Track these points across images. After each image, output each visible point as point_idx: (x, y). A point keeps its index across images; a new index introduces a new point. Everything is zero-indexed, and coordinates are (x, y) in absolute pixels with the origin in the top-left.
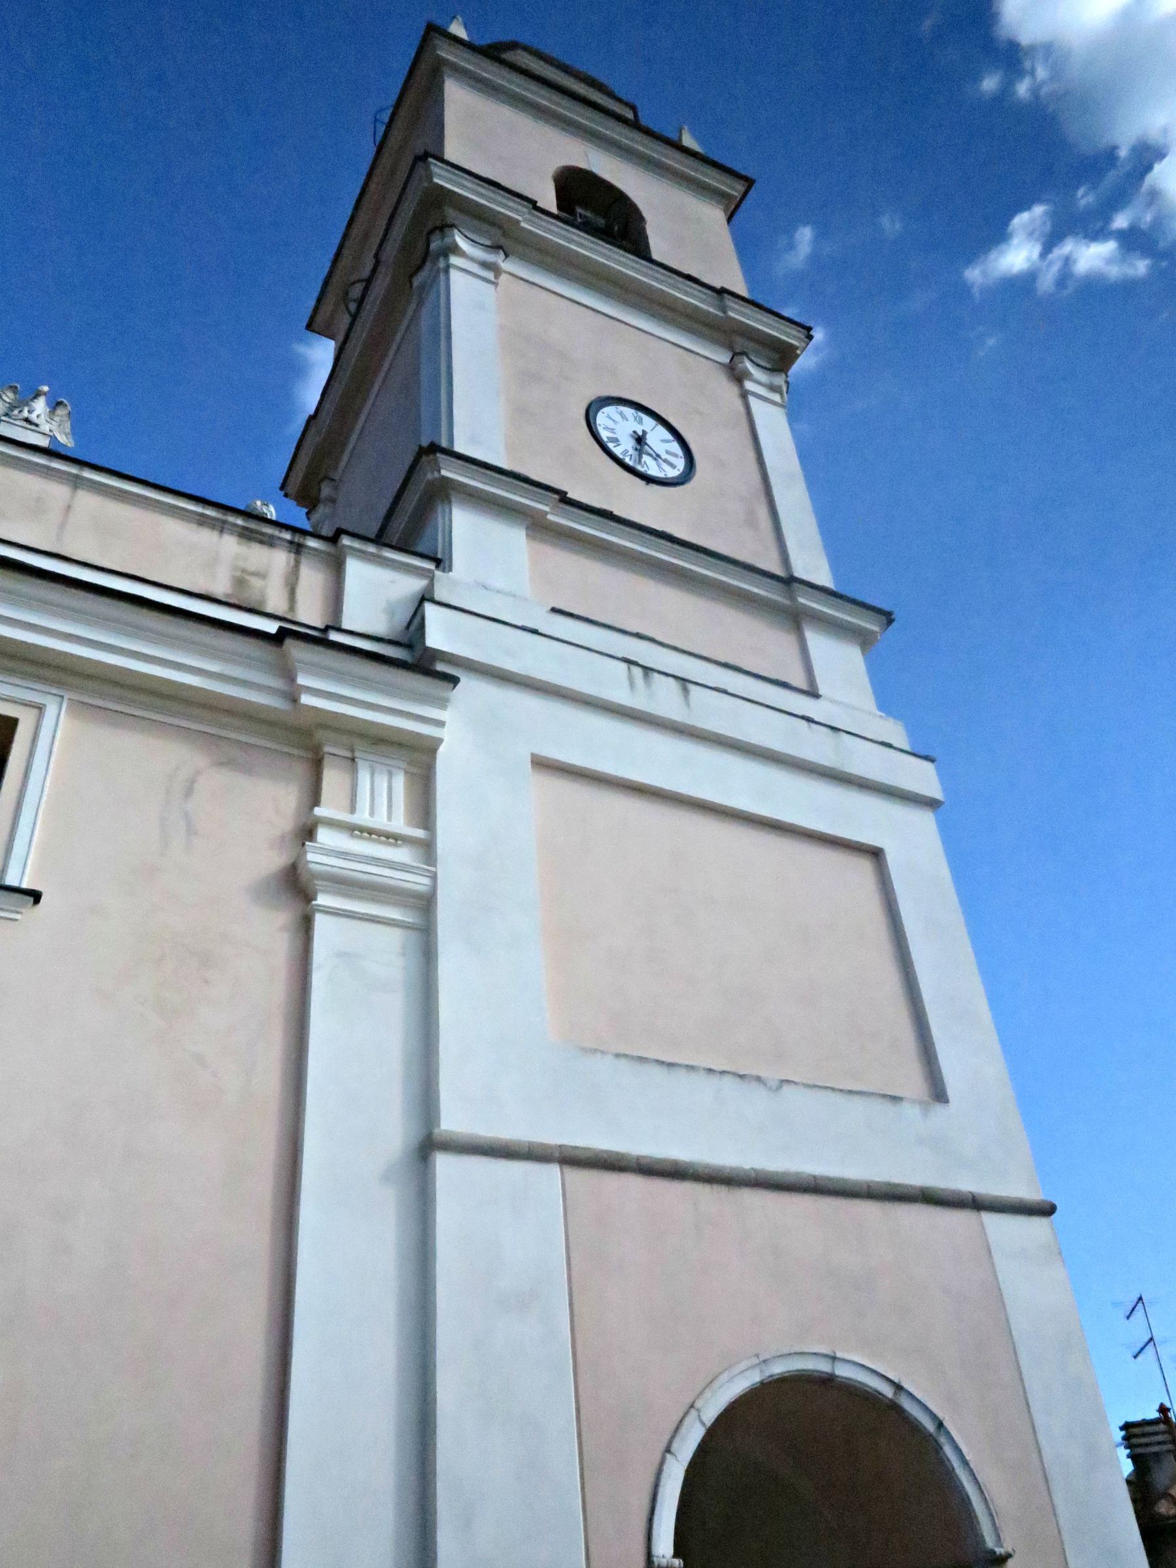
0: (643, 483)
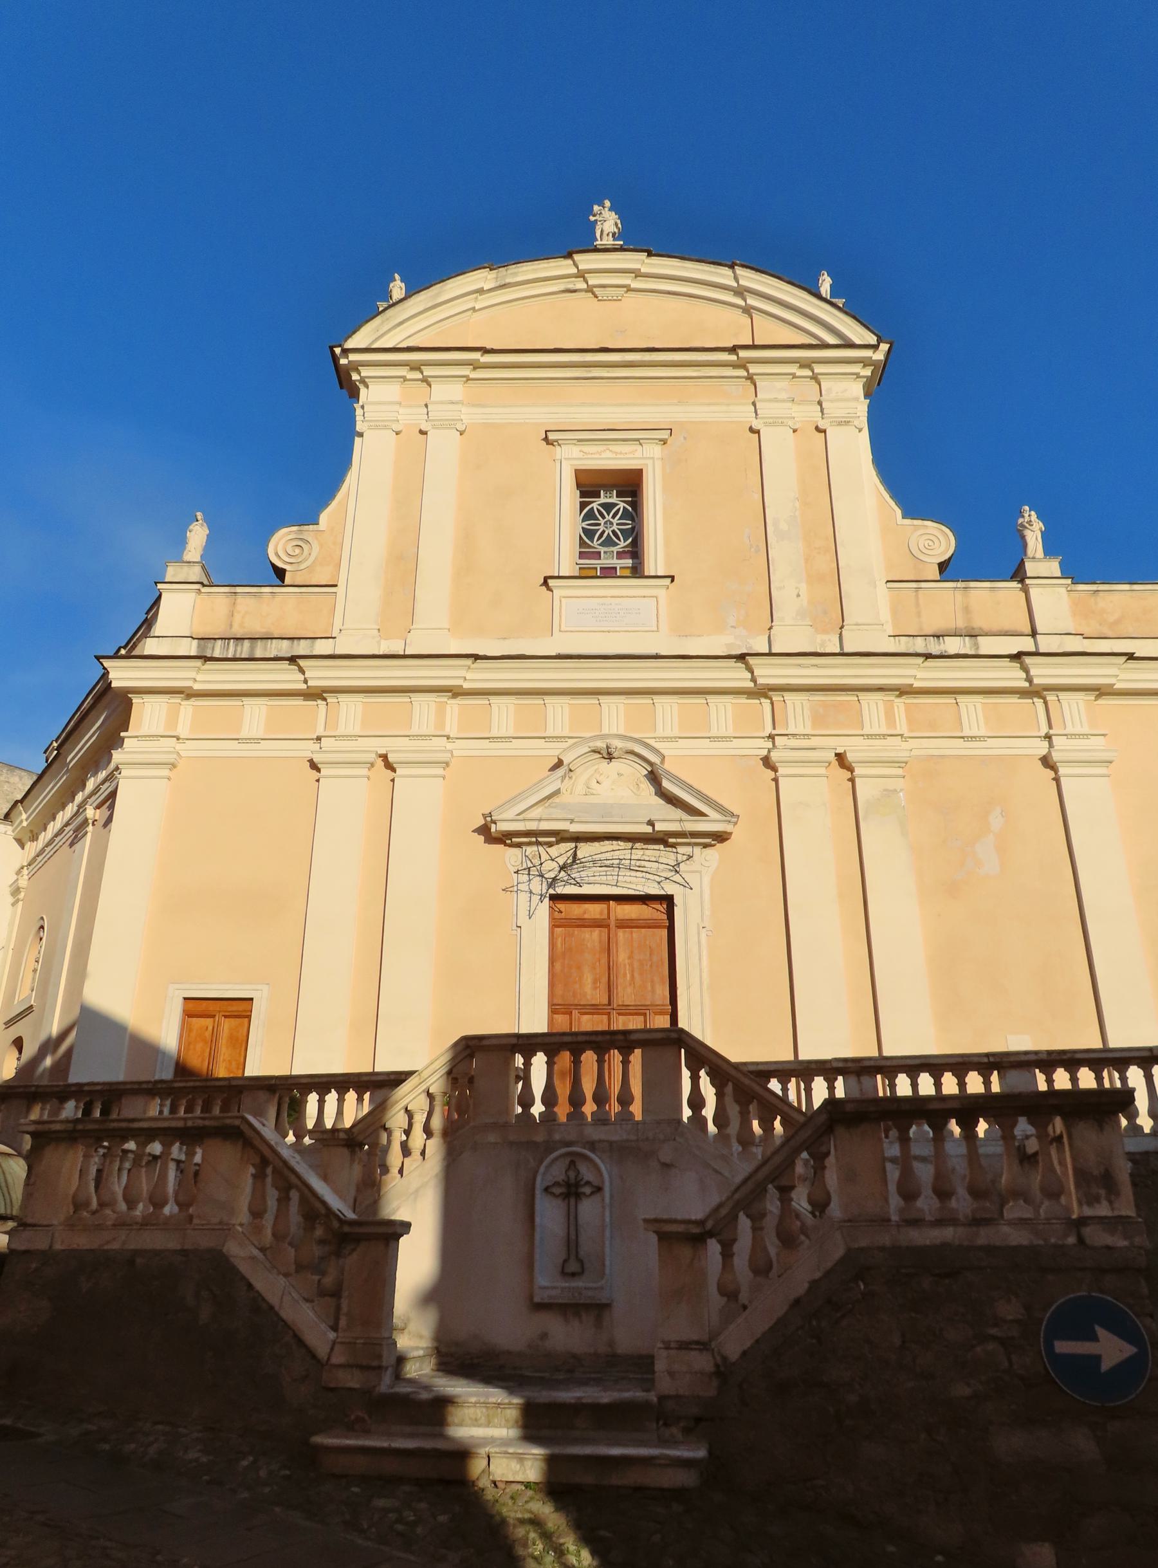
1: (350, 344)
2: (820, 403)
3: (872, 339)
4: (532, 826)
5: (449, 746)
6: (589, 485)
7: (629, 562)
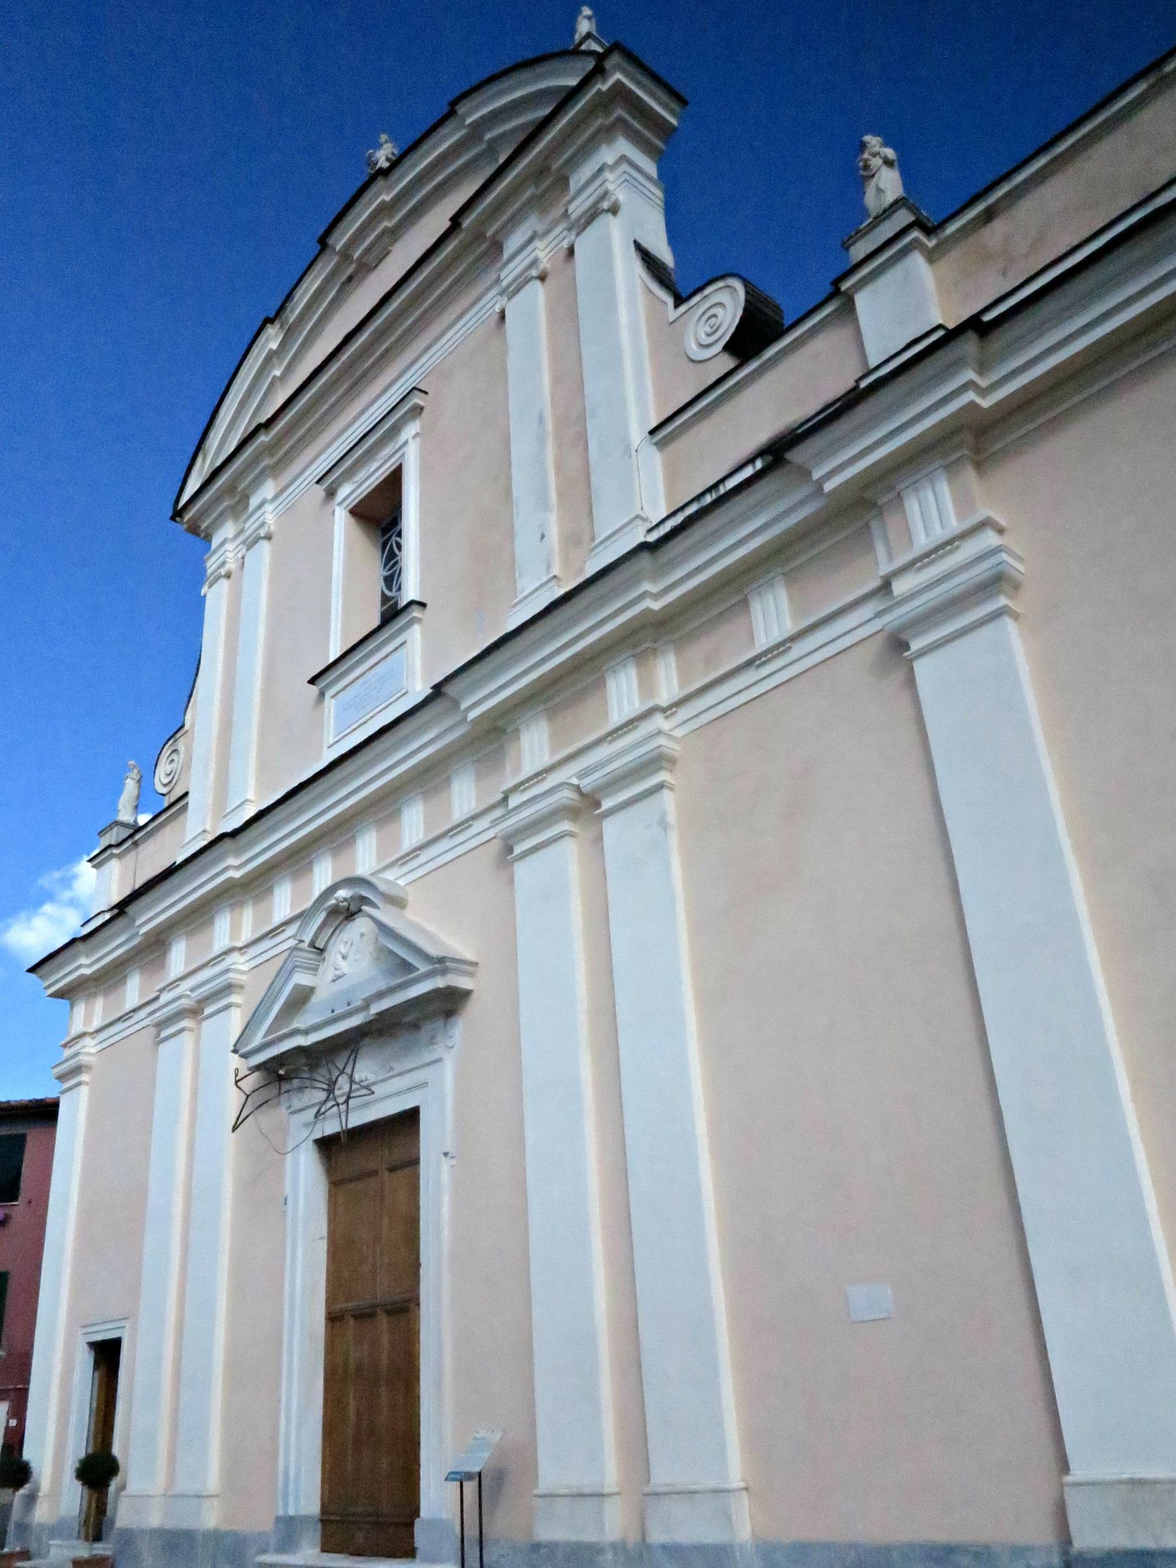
1: (181, 504)
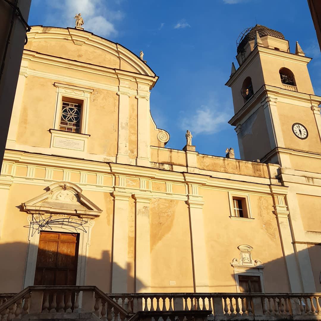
0: (301, 140)
2: (137, 90)
3: (154, 75)
4: (38, 208)
5: (12, 179)
6: (66, 101)
7: (75, 127)
